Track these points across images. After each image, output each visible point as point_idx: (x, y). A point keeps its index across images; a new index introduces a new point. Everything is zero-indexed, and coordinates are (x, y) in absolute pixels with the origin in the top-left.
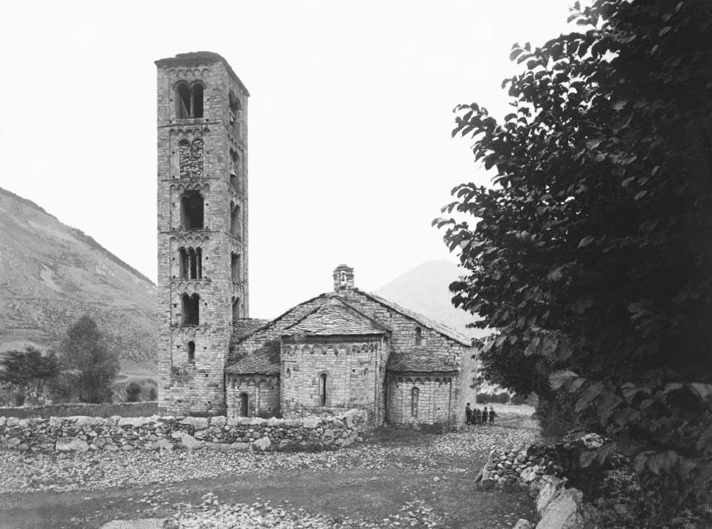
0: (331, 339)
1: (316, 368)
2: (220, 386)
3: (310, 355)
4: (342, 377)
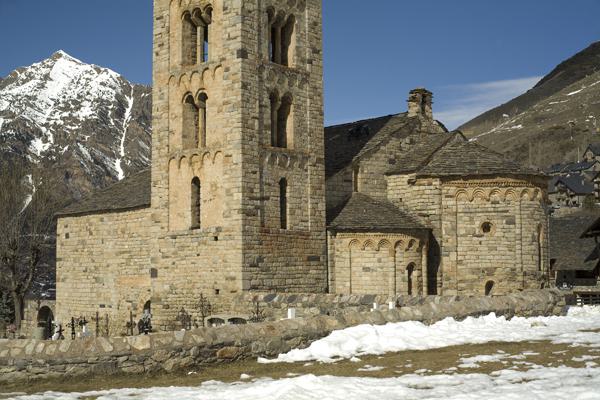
1: (535, 220)
2: (321, 259)
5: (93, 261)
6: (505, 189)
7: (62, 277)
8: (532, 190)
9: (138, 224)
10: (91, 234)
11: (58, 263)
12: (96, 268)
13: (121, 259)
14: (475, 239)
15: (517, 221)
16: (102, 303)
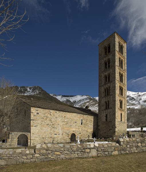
5: (52, 123)
7: (35, 125)
9: (70, 116)
10: (51, 115)
11: (31, 121)
12: (53, 124)
13: (64, 123)
16: (55, 135)
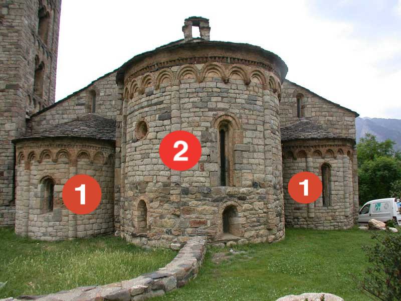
0: (239, 56)
1: (211, 110)
2: (6, 174)
3: (197, 85)
4: (258, 129)
6: (157, 73)
8: (200, 67)
14: (133, 144)
15: (174, 113)
